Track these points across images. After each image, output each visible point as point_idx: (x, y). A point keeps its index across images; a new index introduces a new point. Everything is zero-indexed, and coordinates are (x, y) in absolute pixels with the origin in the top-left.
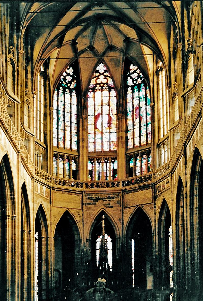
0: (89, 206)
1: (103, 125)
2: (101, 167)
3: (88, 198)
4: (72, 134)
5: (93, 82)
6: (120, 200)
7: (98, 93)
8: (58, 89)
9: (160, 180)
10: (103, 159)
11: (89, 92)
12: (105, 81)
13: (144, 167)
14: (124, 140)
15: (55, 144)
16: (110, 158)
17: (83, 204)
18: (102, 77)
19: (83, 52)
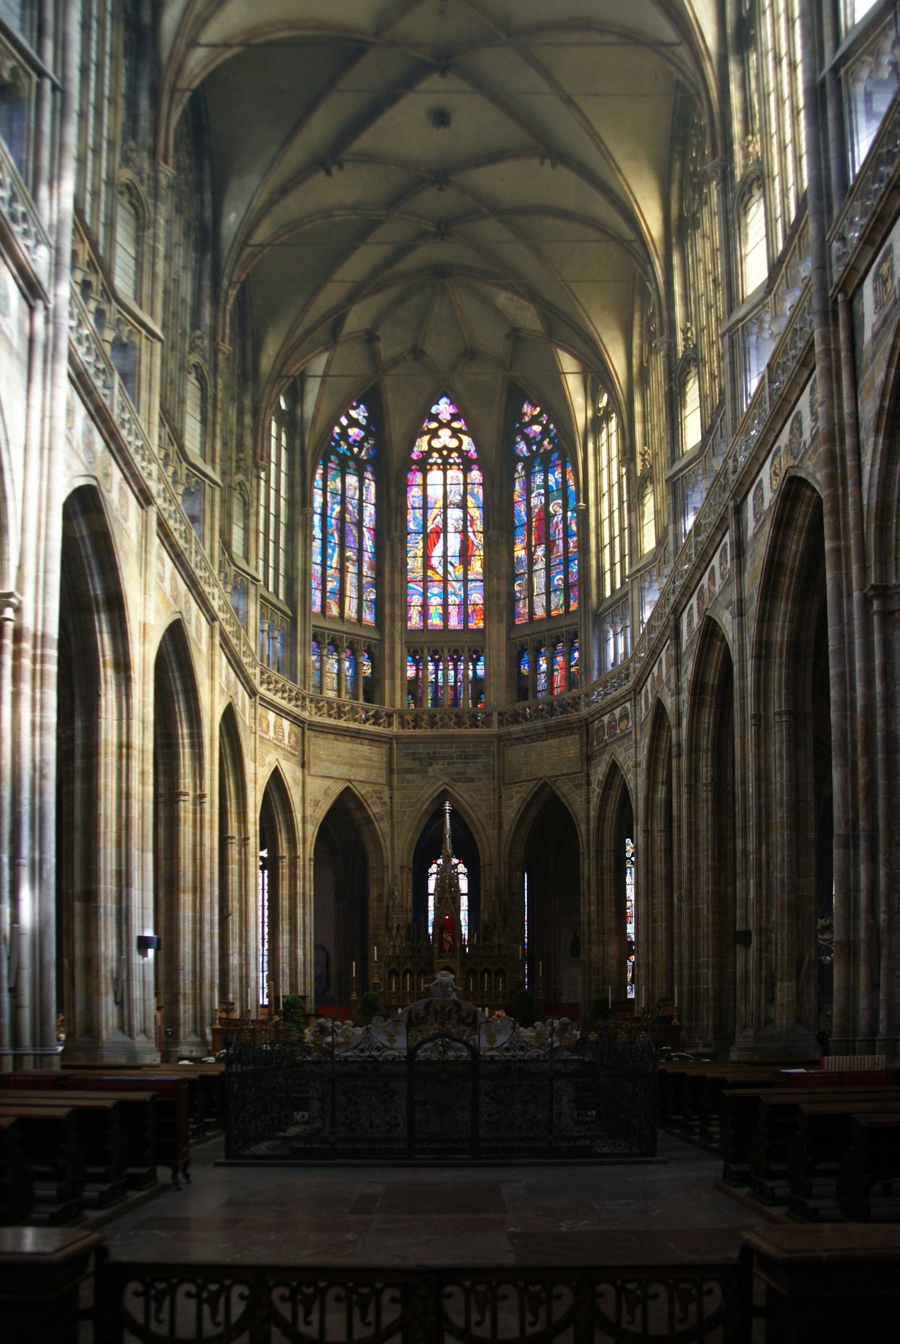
0: (409, 776)
1: (449, 559)
2: (440, 673)
3: (406, 754)
4: (365, 581)
5: (422, 444)
6: (491, 762)
7: (435, 476)
8: (326, 461)
9: (602, 711)
10: (446, 651)
11: (412, 470)
12: (454, 443)
13: (558, 676)
14: (503, 601)
15: (317, 608)
16: (466, 650)
17: (390, 771)
18: (445, 433)
19: (395, 362)
